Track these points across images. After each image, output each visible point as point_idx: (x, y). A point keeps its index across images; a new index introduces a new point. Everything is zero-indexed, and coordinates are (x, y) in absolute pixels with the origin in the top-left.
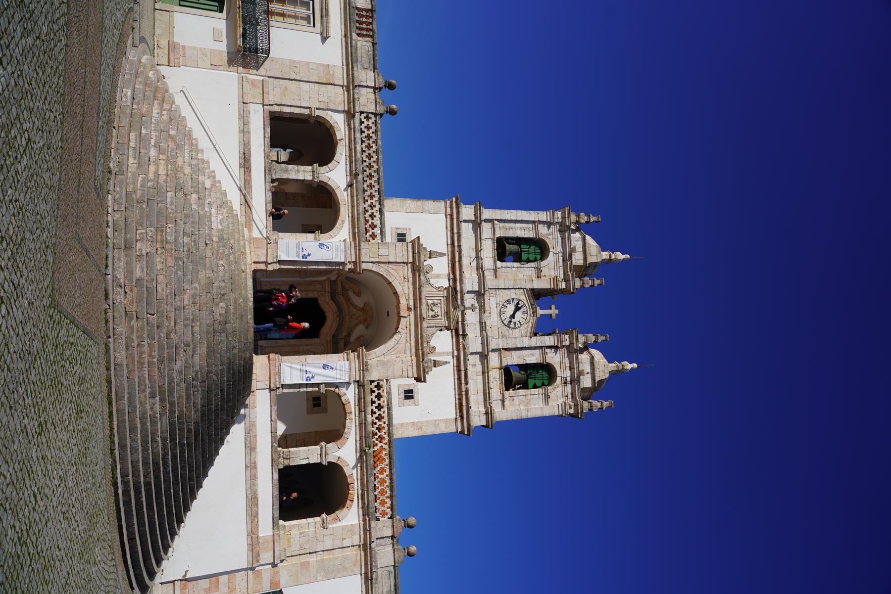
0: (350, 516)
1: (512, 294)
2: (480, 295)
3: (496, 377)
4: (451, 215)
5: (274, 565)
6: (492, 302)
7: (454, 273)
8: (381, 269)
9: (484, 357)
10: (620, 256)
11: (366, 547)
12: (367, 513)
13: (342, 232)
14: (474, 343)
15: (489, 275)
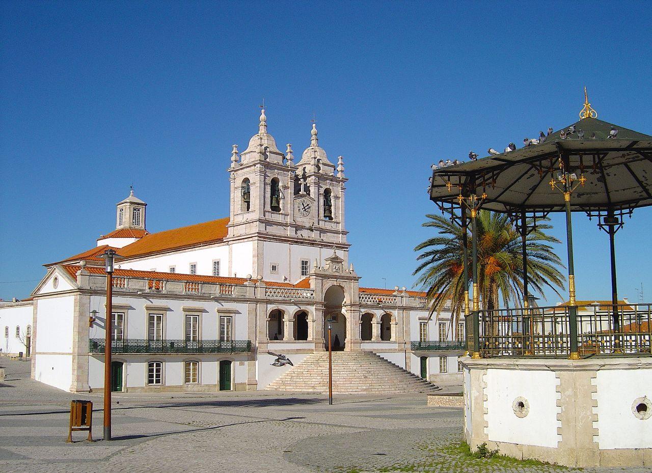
0: (395, 313)
1: (296, 206)
2: (298, 228)
3: (328, 226)
4: (264, 238)
5: (405, 343)
6: (300, 220)
7: (288, 241)
8: (324, 291)
9: (323, 231)
10: (263, 117)
11: (404, 308)
12: (394, 308)
13: (312, 309)
14: (314, 235)
15: (289, 220)
